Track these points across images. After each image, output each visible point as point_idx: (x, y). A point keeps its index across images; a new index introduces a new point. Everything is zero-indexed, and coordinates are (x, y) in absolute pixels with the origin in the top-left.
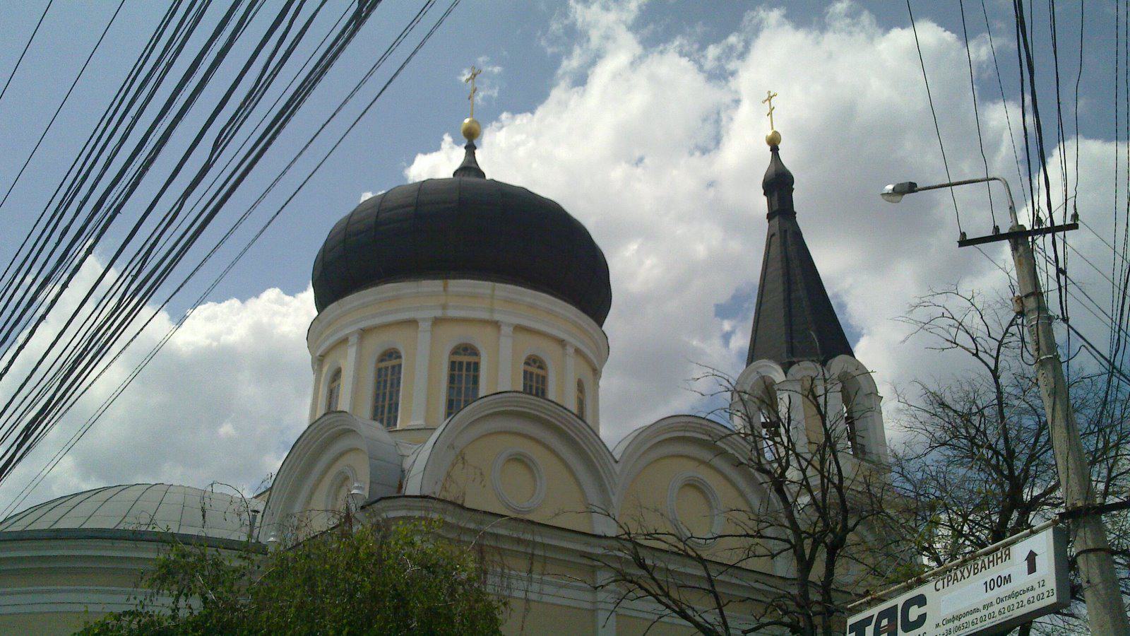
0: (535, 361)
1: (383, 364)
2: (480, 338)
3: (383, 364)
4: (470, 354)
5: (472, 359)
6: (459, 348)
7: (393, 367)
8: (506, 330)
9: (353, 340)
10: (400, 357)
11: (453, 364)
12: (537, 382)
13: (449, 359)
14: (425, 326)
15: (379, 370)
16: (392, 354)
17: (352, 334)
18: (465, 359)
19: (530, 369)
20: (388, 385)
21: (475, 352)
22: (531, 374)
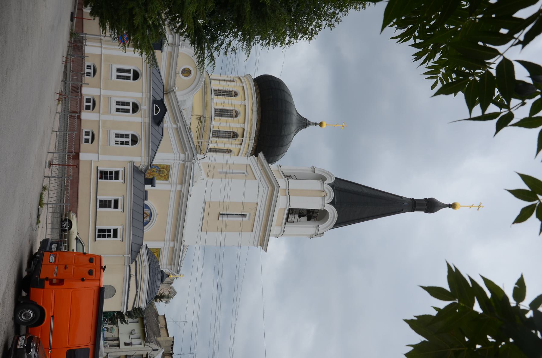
0: (235, 135)
1: (233, 93)
2: (241, 118)
3: (233, 93)
7: (232, 95)
10: (235, 96)
11: (233, 110)
12: (228, 136)
14: (243, 103)
15: (232, 92)
16: (236, 94)
18: (234, 114)
20: (227, 94)
21: (236, 117)
22: (231, 134)
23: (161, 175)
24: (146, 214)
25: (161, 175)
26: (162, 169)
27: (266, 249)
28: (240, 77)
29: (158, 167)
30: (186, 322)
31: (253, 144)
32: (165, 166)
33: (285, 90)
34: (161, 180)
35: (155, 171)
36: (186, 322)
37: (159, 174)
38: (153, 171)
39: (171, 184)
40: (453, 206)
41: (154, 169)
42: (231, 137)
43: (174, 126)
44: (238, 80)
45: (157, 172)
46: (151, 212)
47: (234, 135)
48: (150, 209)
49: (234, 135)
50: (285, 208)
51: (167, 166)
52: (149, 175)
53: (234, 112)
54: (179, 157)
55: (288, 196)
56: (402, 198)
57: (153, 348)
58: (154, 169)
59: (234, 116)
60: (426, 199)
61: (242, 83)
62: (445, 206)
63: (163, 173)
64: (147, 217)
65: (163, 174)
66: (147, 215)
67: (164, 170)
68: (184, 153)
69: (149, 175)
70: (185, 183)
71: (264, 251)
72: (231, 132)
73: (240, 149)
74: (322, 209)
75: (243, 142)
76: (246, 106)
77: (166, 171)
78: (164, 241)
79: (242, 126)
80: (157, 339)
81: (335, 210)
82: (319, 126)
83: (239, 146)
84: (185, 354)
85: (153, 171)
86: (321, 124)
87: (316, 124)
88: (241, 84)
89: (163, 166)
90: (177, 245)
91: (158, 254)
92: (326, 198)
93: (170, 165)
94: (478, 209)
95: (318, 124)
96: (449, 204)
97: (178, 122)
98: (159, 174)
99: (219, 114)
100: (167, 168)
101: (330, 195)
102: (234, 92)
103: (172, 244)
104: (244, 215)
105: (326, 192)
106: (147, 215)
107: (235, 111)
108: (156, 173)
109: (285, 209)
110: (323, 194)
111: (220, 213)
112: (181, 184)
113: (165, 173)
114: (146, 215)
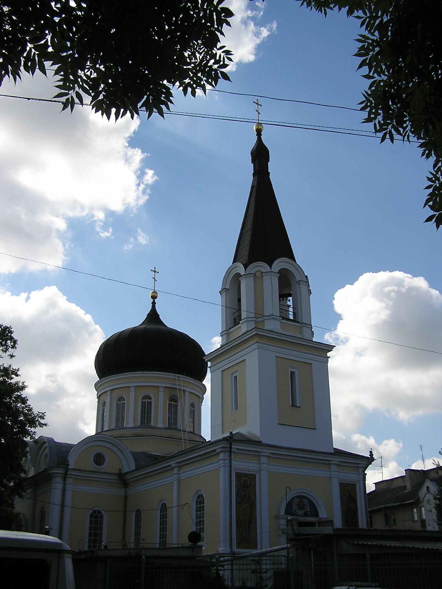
0: (174, 399)
1: (119, 402)
4: (148, 399)
5: (149, 400)
6: (145, 397)
7: (123, 403)
8: (161, 389)
9: (109, 393)
11: (143, 402)
12: (174, 407)
13: (141, 400)
14: (133, 389)
16: (121, 399)
17: (108, 391)
18: (146, 400)
19: (171, 403)
21: (150, 399)
22: (172, 404)
23: (248, 484)
25: (248, 484)
26: (242, 483)
27: (331, 347)
28: (98, 396)
30: (381, 457)
31: (185, 376)
32: (237, 479)
33: (115, 338)
36: (381, 457)
39: (260, 470)
40: (259, 132)
42: (176, 403)
43: (176, 471)
44: (102, 398)
47: (173, 399)
49: (173, 399)
50: (280, 322)
51: (236, 477)
53: (144, 400)
54: (225, 460)
55: (264, 318)
56: (255, 186)
57: (426, 492)
59: (149, 400)
60: (253, 161)
61: (106, 392)
62: (259, 141)
68: (218, 454)
70: (258, 451)
71: (333, 349)
72: (169, 404)
73: (190, 392)
74: (278, 275)
75: (182, 388)
76: (137, 385)
77: (243, 478)
78: (330, 478)
79: (161, 389)
80: (409, 489)
81: (278, 260)
82: (155, 300)
83: (187, 394)
84: (423, 456)
86: (154, 297)
87: (154, 303)
88: (109, 393)
90: (335, 461)
92: (263, 270)
94: (260, 105)
95: (154, 301)
96: (257, 135)
97: (170, 466)
99: (147, 419)
101: (261, 266)
102: (118, 401)
103: (334, 468)
104: (292, 373)
105: (256, 272)
107: (143, 399)
109: (281, 322)
110: (258, 274)
111: (291, 405)
112: (259, 456)
114: (301, 503)
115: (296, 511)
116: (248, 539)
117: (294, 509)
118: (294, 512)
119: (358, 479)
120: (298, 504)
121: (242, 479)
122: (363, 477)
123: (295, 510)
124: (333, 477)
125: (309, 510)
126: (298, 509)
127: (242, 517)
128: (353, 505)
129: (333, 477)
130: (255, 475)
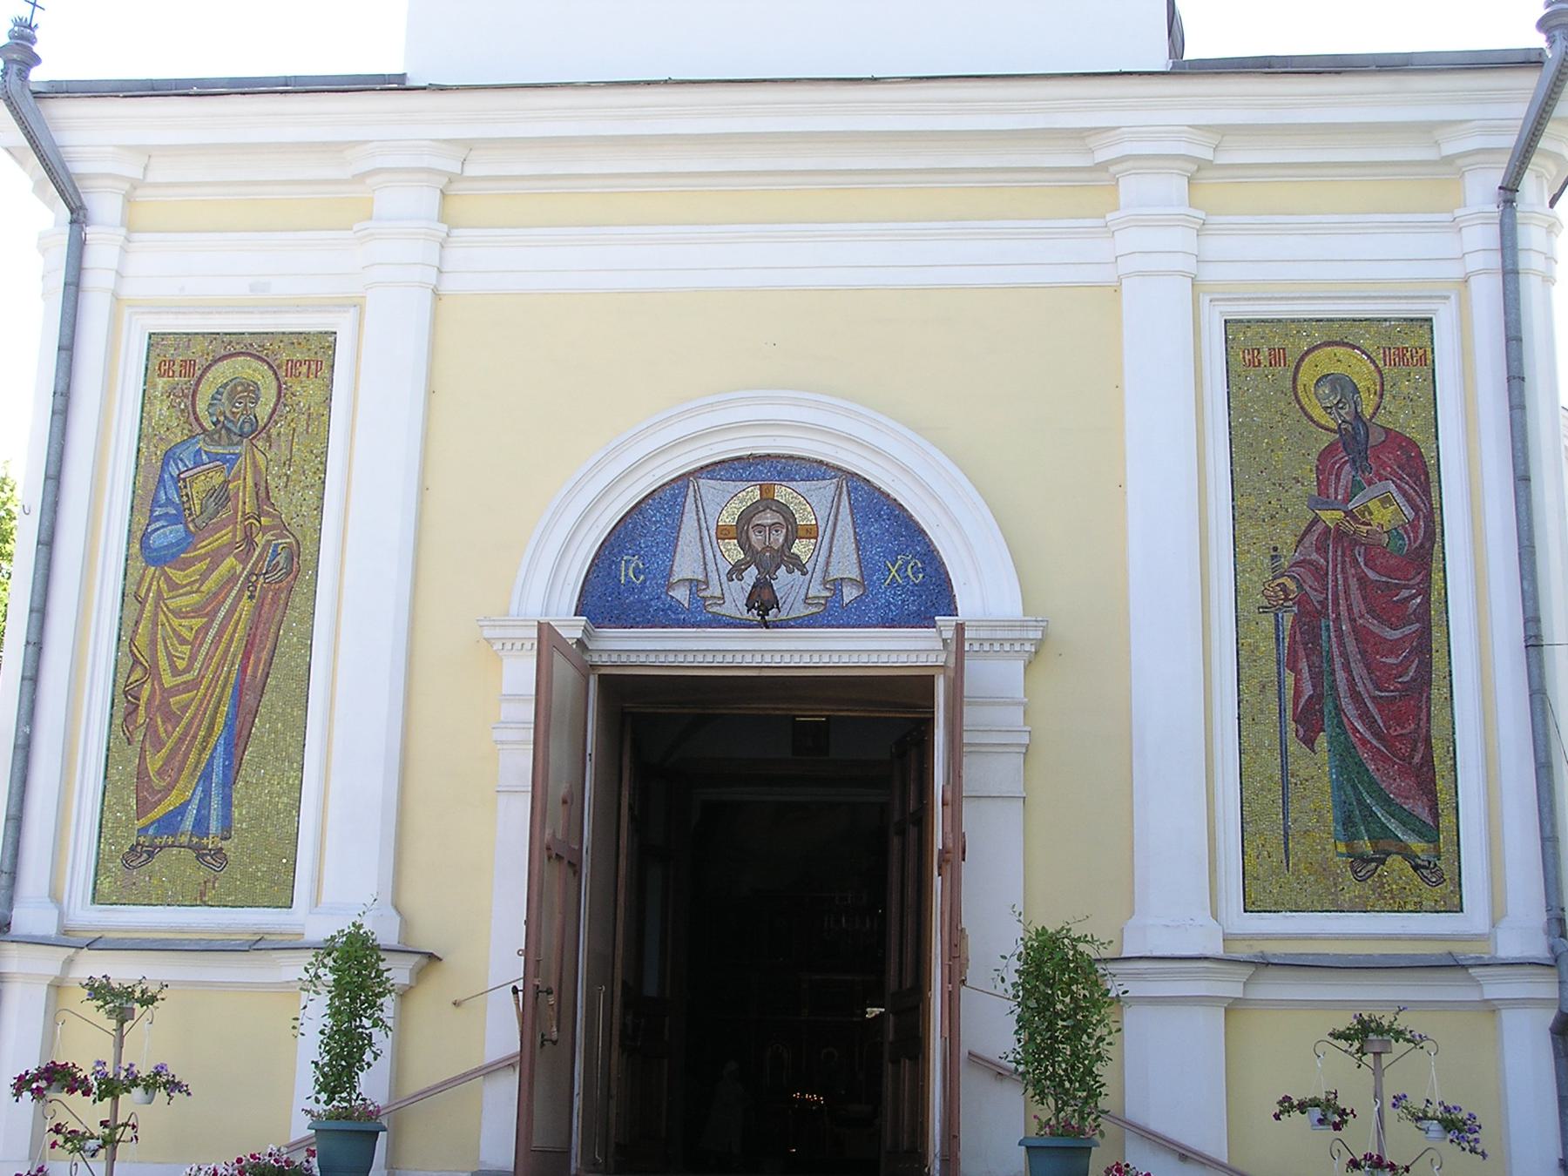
23: (263, 411)
24: (746, 517)
25: (263, 411)
26: (201, 406)
29: (168, 457)
32: (161, 382)
34: (328, 400)
35: (218, 479)
37: (253, 431)
38: (222, 496)
41: (198, 489)
45: (228, 461)
46: (712, 470)
48: (683, 481)
52: (264, 530)
58: (198, 489)
63: (251, 391)
64: (783, 509)
65: (256, 401)
66: (767, 502)
67: (206, 391)
69: (260, 540)
77: (223, 373)
85: (222, 496)
89: (161, 409)
91: (1318, 337)
93: (155, 340)
98: (253, 431)
100: (188, 365)
106: (767, 502)
108: (244, 463)
113: (247, 374)
114: (768, 518)
115: (707, 583)
116: (214, 825)
117: (686, 565)
118: (681, 594)
119: (1454, 271)
120: (741, 530)
121: (209, 375)
122: (1496, 244)
123: (701, 577)
124: (1128, 275)
125: (846, 564)
126: (725, 568)
127: (181, 665)
128: (1386, 501)
129: (1128, 275)
130: (325, 343)
